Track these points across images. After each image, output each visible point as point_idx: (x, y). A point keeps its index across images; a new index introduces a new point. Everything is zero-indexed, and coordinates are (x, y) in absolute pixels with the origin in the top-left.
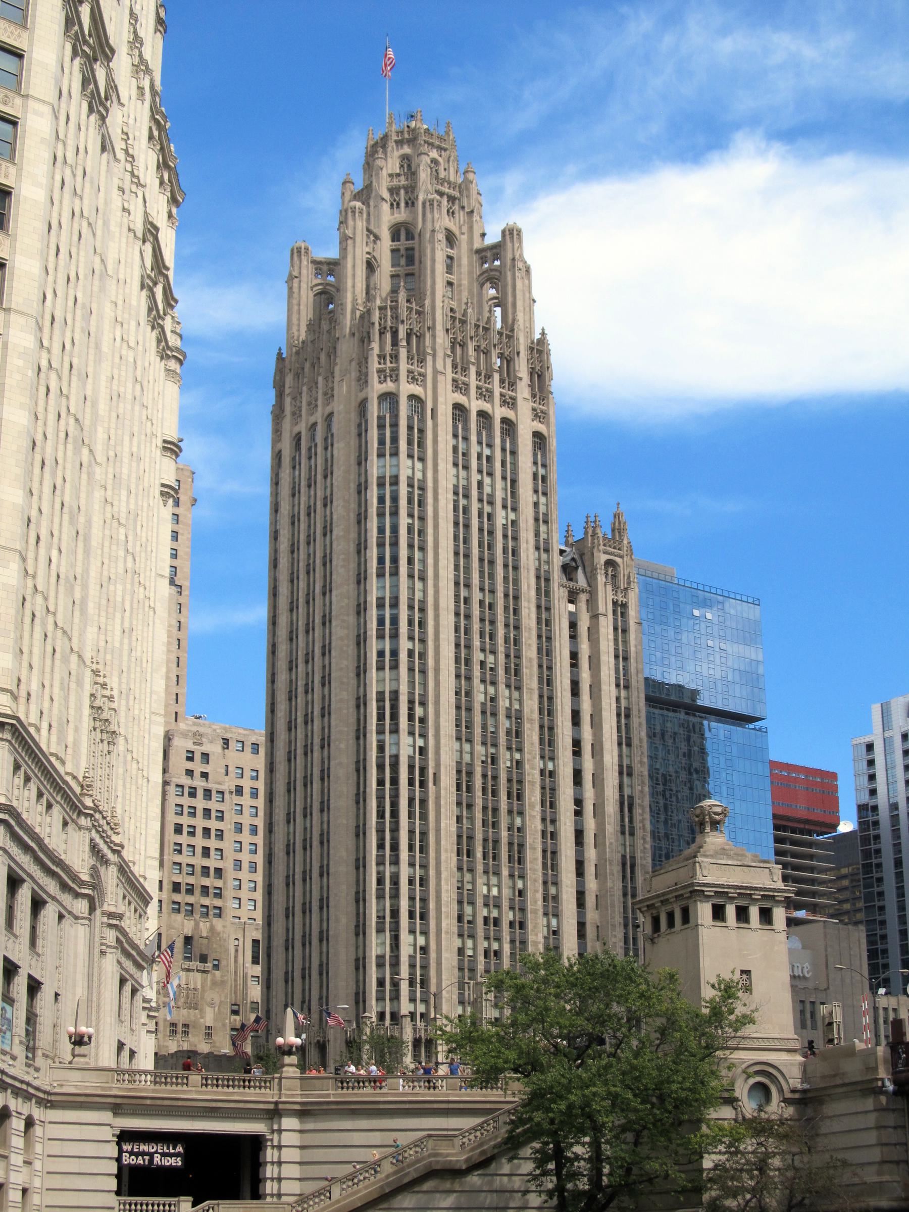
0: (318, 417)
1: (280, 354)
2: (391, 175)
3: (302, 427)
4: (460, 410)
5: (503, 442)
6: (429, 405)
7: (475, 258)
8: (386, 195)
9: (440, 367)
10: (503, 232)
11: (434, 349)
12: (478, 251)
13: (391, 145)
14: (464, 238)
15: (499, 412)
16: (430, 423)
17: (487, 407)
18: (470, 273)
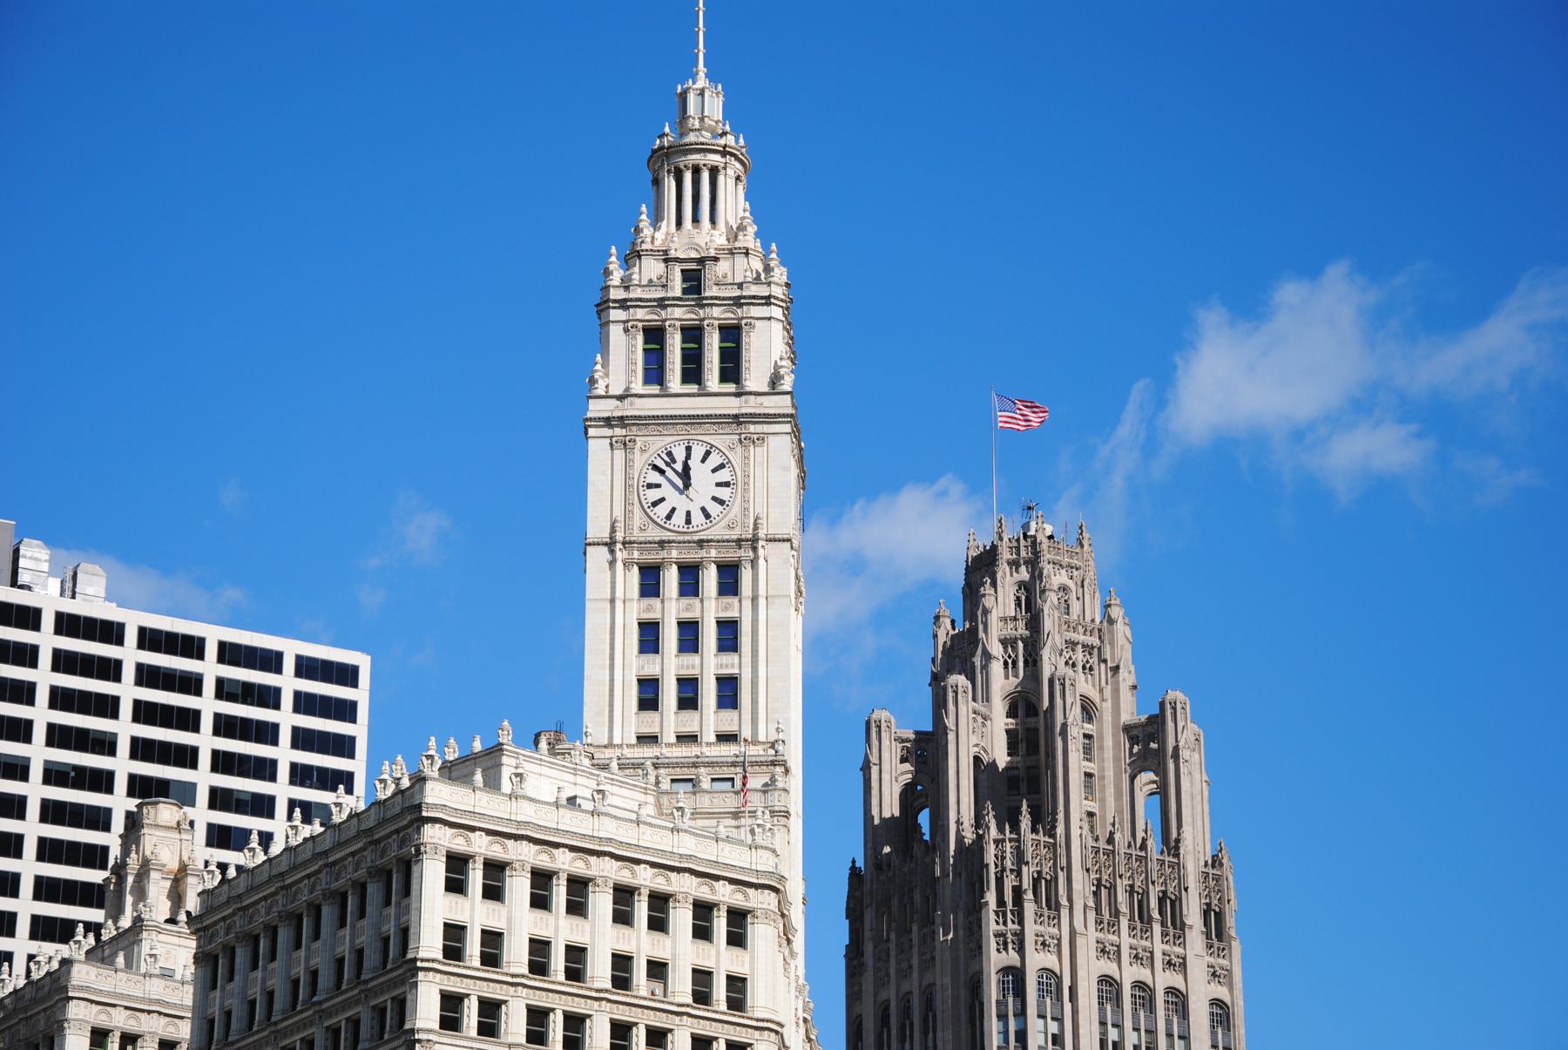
0: (914, 984)
1: (853, 868)
2: (1004, 619)
3: (891, 994)
4: (1109, 985)
5: (1169, 1023)
6: (1066, 982)
7: (1122, 737)
8: (996, 649)
9: (1079, 925)
10: (1162, 705)
11: (1070, 900)
12: (1127, 729)
13: (1003, 569)
14: (1108, 706)
15: (1164, 980)
16: (1068, 1006)
17: (1144, 974)
18: (1117, 759)
